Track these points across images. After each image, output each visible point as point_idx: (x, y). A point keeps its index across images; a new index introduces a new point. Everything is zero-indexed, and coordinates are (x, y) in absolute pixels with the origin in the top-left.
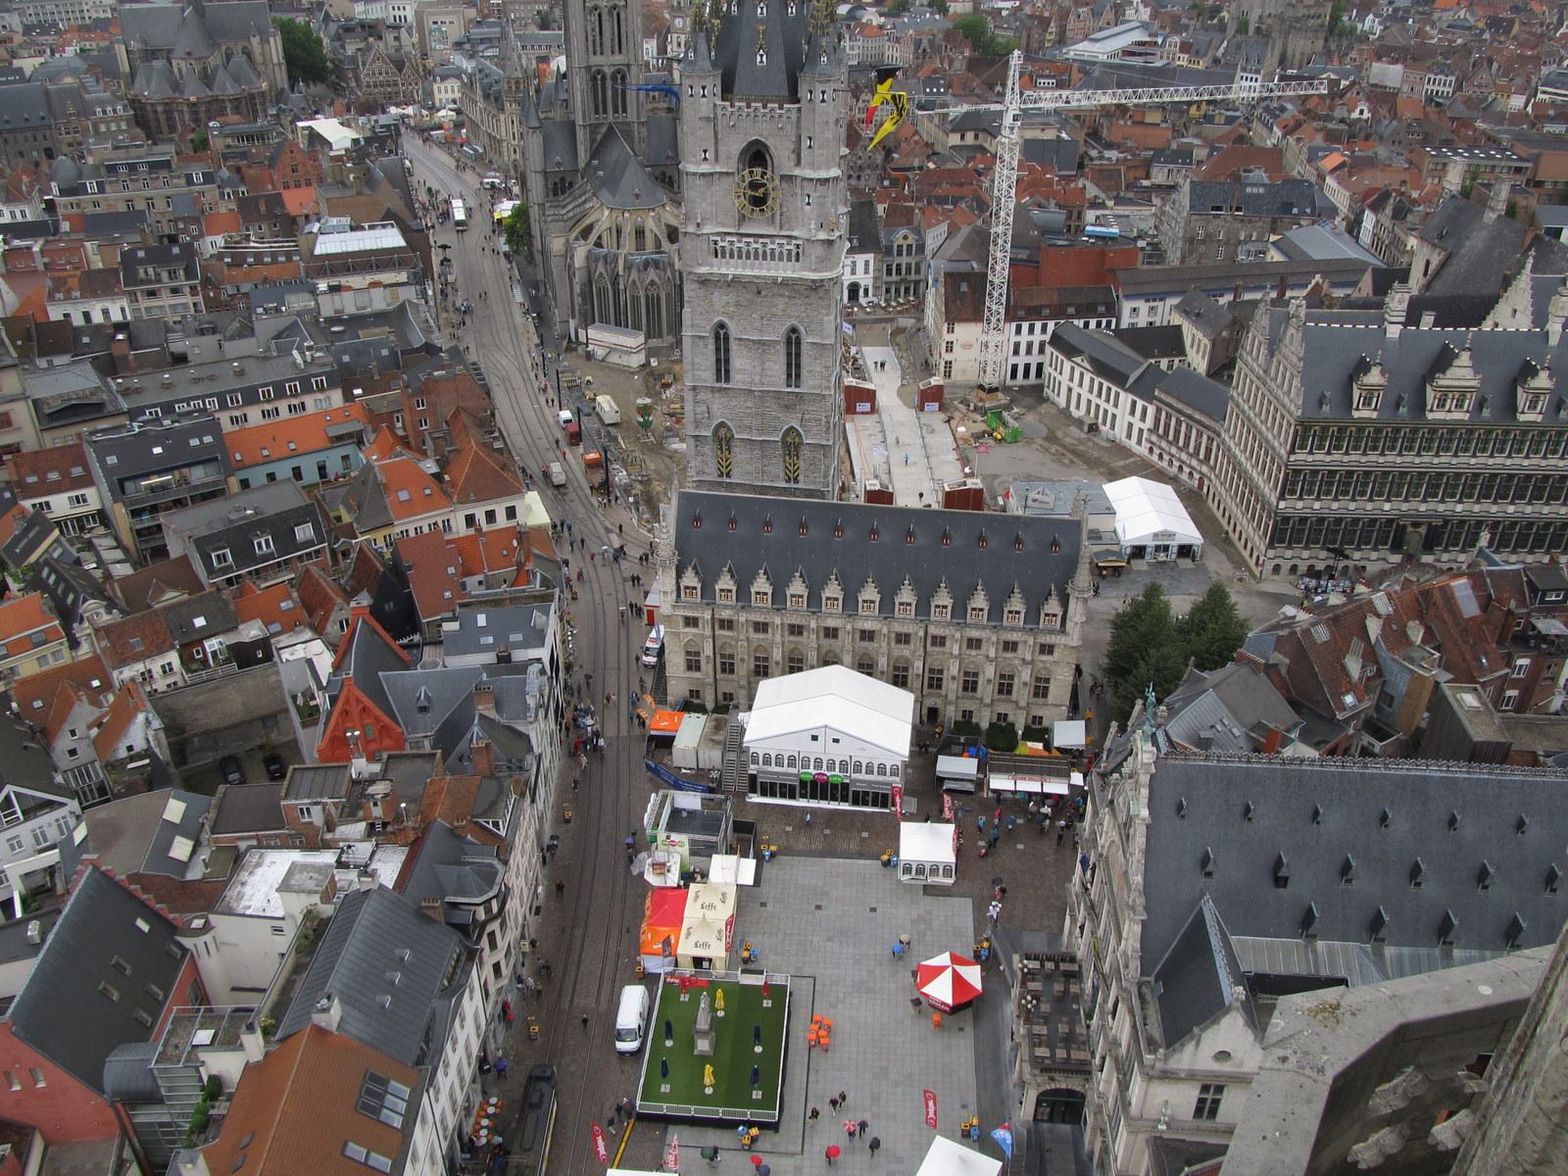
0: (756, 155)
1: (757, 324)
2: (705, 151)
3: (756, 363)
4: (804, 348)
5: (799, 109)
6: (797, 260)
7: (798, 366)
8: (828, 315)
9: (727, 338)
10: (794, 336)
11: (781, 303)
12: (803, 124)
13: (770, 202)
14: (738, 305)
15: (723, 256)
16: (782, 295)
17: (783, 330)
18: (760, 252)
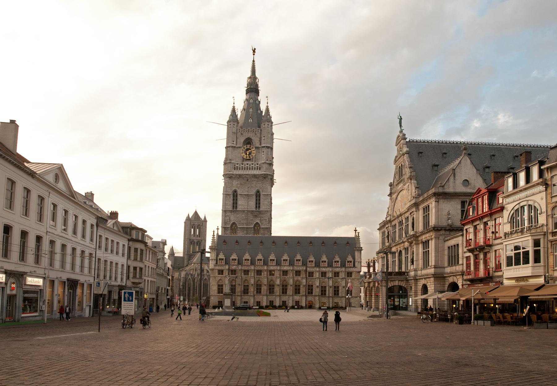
0: (248, 141)
1: (247, 190)
2: (233, 141)
3: (246, 202)
4: (261, 196)
5: (261, 130)
6: (260, 170)
7: (259, 203)
8: (269, 186)
9: (237, 194)
10: (258, 194)
11: (254, 183)
13: (252, 154)
14: (241, 184)
15: (237, 170)
16: (255, 181)
17: (255, 191)
18: (249, 167)
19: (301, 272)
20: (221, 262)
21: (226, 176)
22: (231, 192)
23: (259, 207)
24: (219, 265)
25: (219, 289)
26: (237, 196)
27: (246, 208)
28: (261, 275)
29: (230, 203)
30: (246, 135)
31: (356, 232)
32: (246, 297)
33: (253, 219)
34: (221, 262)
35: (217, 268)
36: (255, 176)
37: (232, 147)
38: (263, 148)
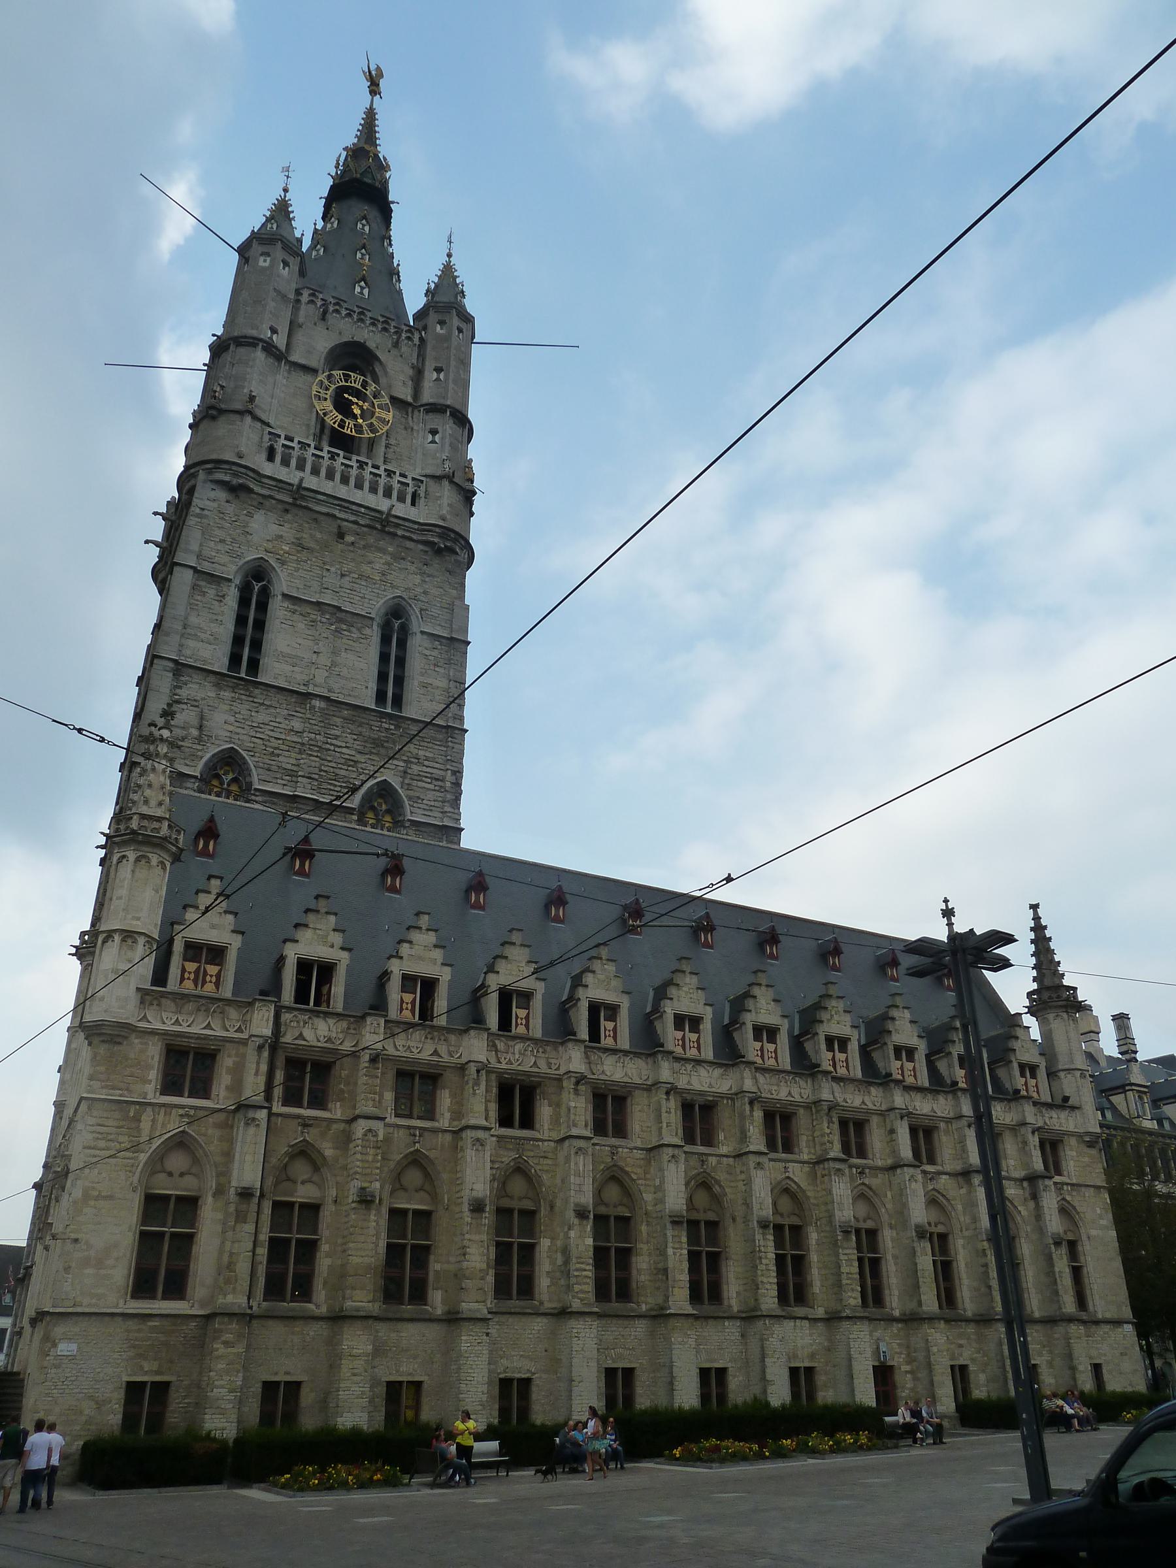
1: (331, 580)
2: (274, 331)
4: (417, 644)
6: (413, 504)
7: (399, 681)
9: (265, 594)
10: (397, 624)
11: (379, 561)
12: (430, 352)
14: (300, 546)
16: (383, 551)
18: (354, 472)
19: (802, 1120)
20: (199, 978)
21: (209, 472)
22: (234, 568)
23: (398, 701)
24: (181, 998)
25: (148, 1241)
26: (263, 607)
27: (319, 679)
28: (528, 1122)
29: (214, 627)
30: (346, 330)
31: (949, 919)
32: (411, 1334)
33: (358, 757)
34: (199, 978)
35: (164, 1020)
36: (384, 524)
37: (269, 348)
38: (431, 416)
